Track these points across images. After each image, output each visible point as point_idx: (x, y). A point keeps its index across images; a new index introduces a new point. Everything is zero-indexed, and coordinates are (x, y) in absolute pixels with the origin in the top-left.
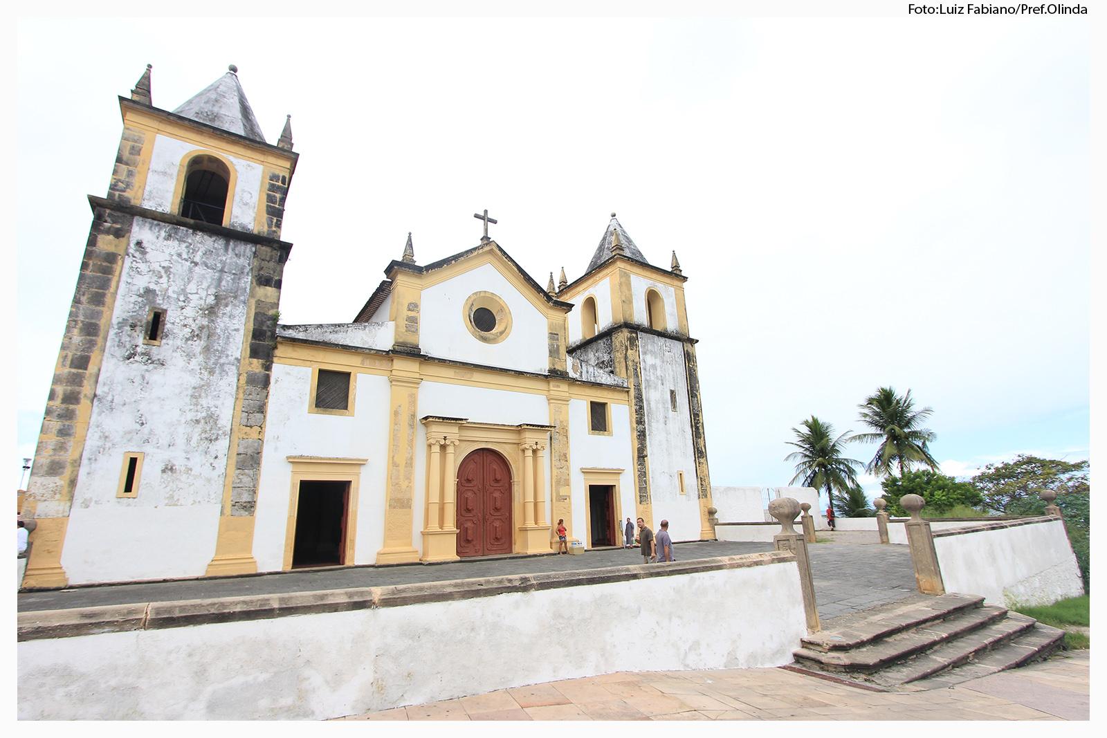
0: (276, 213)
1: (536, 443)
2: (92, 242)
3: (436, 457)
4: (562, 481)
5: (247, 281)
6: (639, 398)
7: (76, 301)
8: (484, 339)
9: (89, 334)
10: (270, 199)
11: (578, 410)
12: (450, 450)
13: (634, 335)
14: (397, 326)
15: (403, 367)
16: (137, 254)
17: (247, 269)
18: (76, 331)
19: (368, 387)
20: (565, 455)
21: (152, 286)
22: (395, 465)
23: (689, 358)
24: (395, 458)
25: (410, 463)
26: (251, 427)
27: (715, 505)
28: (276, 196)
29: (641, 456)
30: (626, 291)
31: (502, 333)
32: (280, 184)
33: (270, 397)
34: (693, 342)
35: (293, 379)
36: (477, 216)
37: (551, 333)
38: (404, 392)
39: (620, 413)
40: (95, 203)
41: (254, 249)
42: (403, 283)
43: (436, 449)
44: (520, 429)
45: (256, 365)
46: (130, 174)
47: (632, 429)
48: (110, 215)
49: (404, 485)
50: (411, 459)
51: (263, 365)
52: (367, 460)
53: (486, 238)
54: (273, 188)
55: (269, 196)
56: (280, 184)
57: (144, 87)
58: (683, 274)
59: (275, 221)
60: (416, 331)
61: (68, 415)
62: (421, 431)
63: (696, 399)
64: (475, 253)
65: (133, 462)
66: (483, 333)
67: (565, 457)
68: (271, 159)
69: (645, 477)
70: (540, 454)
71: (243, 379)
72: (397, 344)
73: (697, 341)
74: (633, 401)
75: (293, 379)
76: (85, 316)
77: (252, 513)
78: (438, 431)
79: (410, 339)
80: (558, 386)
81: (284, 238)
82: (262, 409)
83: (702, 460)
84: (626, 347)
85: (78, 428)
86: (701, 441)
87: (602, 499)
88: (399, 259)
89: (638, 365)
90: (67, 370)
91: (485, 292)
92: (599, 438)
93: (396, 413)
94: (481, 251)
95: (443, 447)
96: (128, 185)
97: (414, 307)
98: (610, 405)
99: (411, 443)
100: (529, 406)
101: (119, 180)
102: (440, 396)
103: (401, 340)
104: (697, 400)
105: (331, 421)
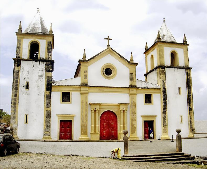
0: (50, 52)
1: (124, 109)
2: (14, 69)
3: (93, 114)
4: (133, 119)
5: (45, 71)
7: (13, 82)
8: (107, 78)
9: (16, 89)
10: (48, 48)
11: (141, 98)
12: (97, 112)
13: (164, 69)
14: (81, 78)
15: (84, 89)
16: (22, 70)
17: (45, 68)
18: (14, 89)
19: (74, 96)
20: (135, 112)
21: (26, 77)
22: (82, 116)
23: (188, 75)
24: (82, 114)
25: (86, 115)
26: (48, 108)
28: (51, 46)
29: (165, 110)
30: (162, 53)
32: (50, 44)
33: (51, 100)
34: (190, 69)
35: (56, 96)
36: (105, 39)
37: (131, 73)
38: (84, 96)
40: (14, 59)
41: (45, 63)
42: (83, 65)
43: (93, 112)
44: (119, 105)
45: (48, 93)
46: (20, 50)
47: (161, 102)
48: (17, 62)
49: (85, 121)
50: (87, 114)
51: (49, 92)
52: (75, 115)
53: (108, 46)
54: (49, 45)
55: (48, 47)
56: (50, 44)
57: (20, 29)
58: (188, 43)
59: (49, 54)
60: (87, 79)
61: (15, 107)
62: (89, 106)
63: (190, 90)
64: (104, 52)
65: (26, 116)
66: (108, 76)
67: (134, 112)
68: (48, 38)
69: (166, 117)
70: (125, 112)
71: (46, 96)
73: (192, 68)
74: (162, 92)
75: (56, 96)
76: (15, 86)
77: (50, 128)
78: (94, 107)
79: (85, 81)
80: (133, 90)
81: (53, 59)
82: (50, 104)
83: (191, 111)
84: (160, 74)
85: (17, 110)
86: (191, 105)
87: (149, 126)
88: (82, 59)
89: (165, 80)
90: (13, 97)
91: (108, 63)
92: (148, 105)
93: (82, 102)
94: (105, 51)
95: (95, 111)
96: (19, 53)
97: (86, 72)
98: (153, 95)
99: (86, 110)
101: (17, 53)
102: (94, 97)
103: (83, 82)
104: (191, 90)
105: (66, 104)
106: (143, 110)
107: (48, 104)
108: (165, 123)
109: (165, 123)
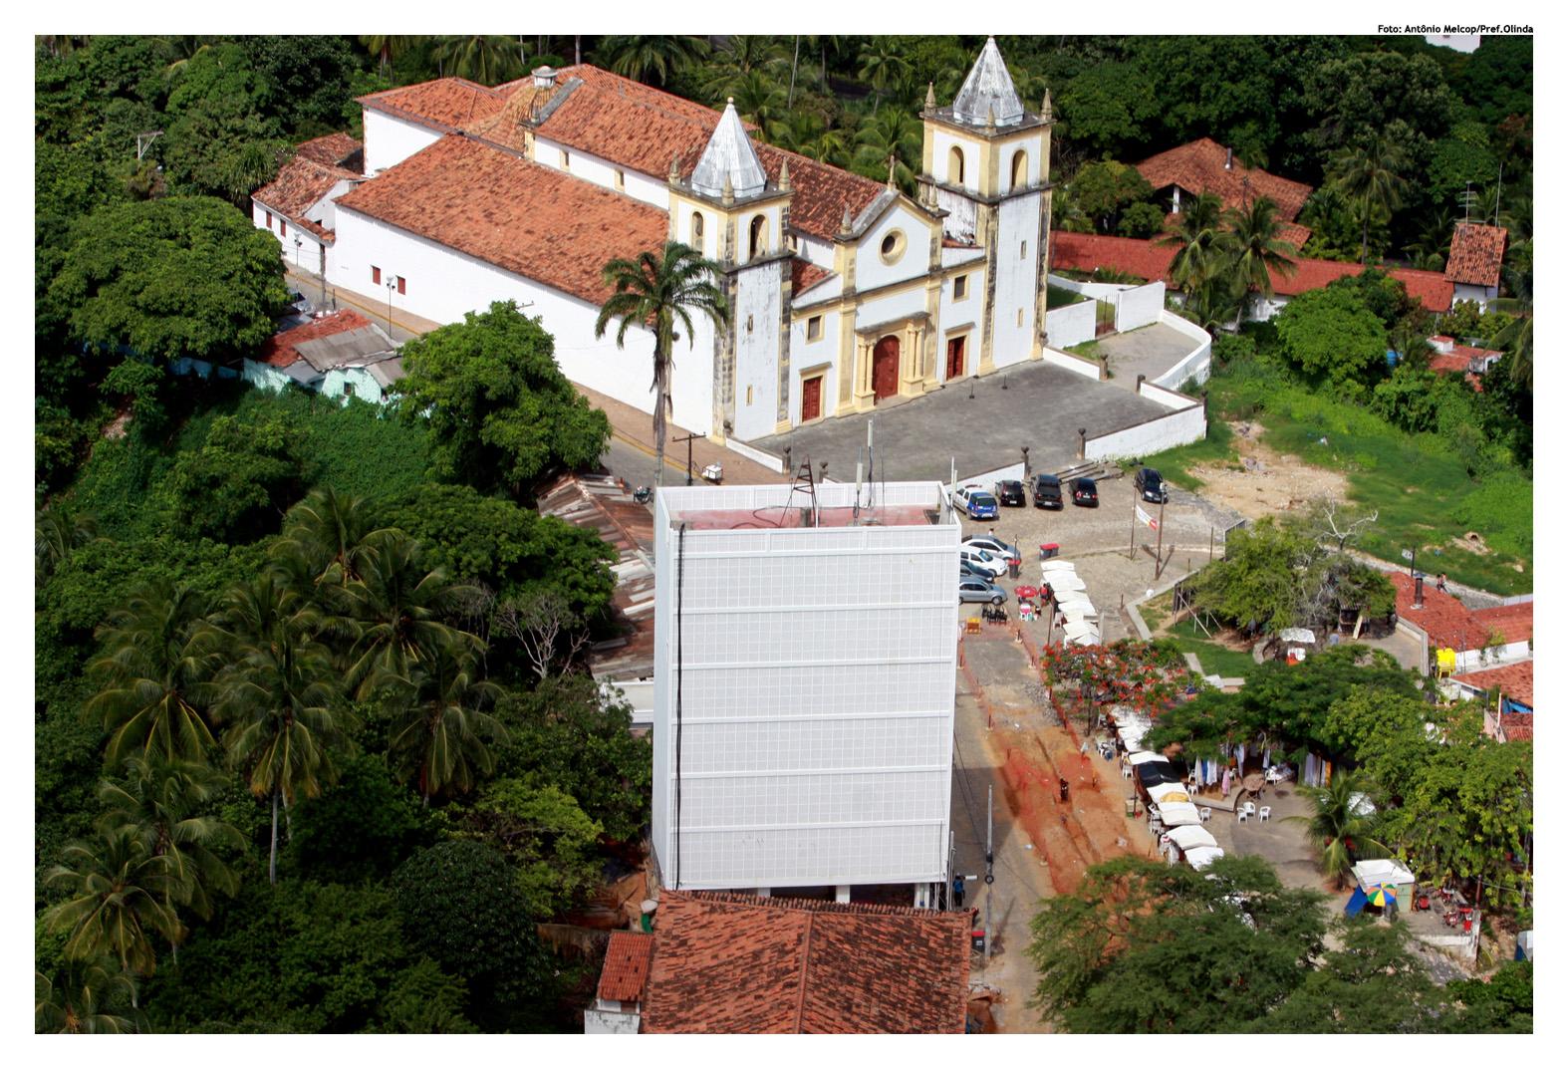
6: (994, 261)
8: (889, 262)
25: (851, 358)
27: (1046, 329)
29: (989, 306)
31: (902, 252)
39: (977, 280)
72: (845, 290)
87: (957, 346)
100: (916, 300)
105: (815, 345)
106: (951, 314)
107: (786, 352)
108: (987, 333)
109: (987, 333)
